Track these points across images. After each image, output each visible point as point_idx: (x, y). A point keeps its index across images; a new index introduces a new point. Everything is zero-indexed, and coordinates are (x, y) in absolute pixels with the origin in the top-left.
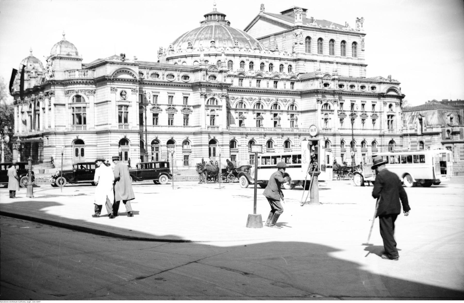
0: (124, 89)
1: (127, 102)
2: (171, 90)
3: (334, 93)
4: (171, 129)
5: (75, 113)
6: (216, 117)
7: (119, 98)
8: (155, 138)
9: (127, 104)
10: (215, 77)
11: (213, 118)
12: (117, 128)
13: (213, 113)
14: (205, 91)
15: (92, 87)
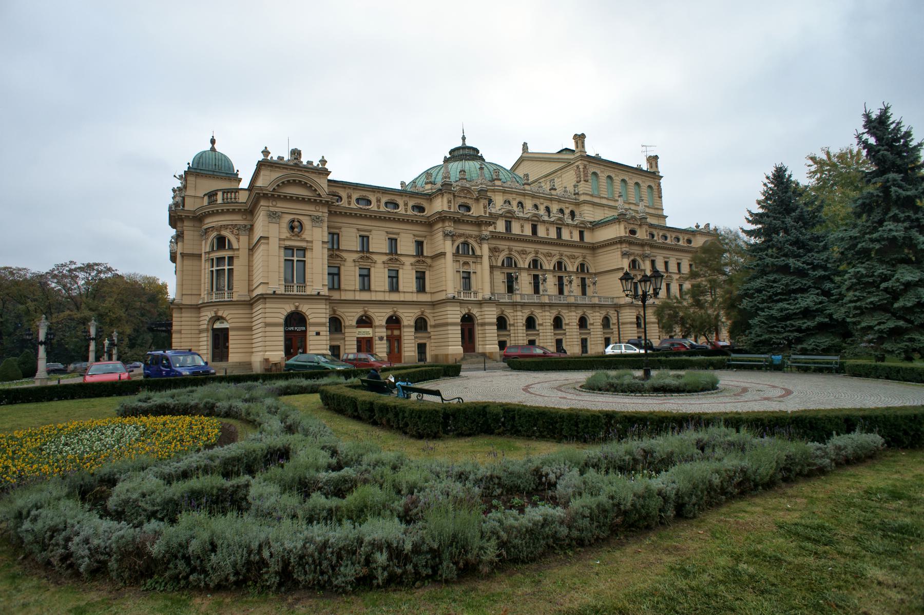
0: (297, 217)
1: (304, 240)
2: (394, 227)
3: (642, 244)
4: (394, 297)
5: (214, 269)
6: (473, 276)
7: (286, 233)
8: (362, 313)
9: (303, 244)
10: (468, 208)
11: (467, 278)
12: (281, 290)
13: (466, 269)
14: (452, 229)
15: (245, 219)
